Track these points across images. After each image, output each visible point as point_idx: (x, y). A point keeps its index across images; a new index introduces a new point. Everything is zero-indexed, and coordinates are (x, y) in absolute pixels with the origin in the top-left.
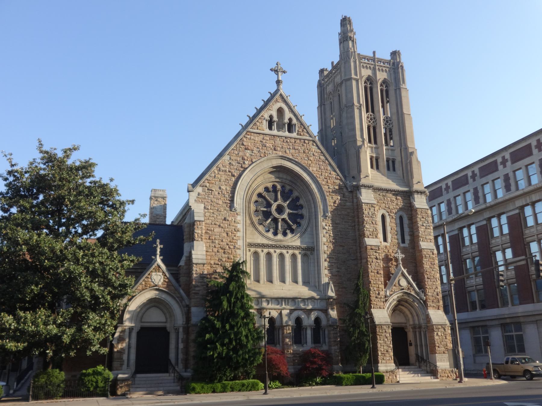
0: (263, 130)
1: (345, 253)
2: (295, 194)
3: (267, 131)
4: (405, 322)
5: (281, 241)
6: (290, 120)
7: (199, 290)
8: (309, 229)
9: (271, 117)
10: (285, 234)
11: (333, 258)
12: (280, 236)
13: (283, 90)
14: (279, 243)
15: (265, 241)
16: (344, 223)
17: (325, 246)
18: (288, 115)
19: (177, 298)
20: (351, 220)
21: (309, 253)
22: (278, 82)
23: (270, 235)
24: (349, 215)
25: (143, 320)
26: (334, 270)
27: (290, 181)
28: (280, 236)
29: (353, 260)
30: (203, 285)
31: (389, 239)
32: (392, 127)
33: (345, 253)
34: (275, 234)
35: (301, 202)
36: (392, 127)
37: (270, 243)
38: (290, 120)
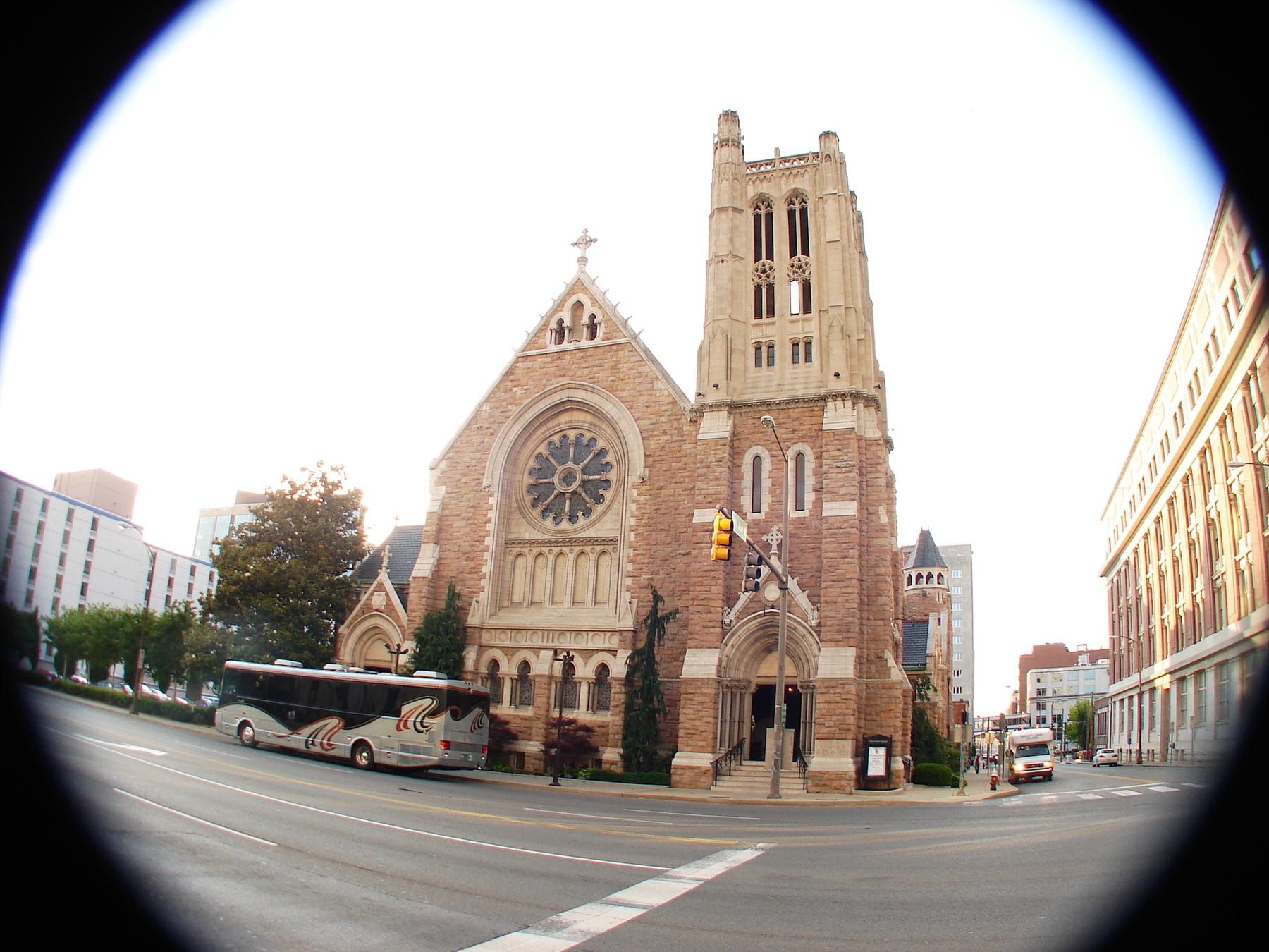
0: (546, 348)
1: (668, 544)
2: (601, 444)
3: (553, 348)
4: (796, 675)
5: (564, 532)
6: (593, 317)
7: (416, 617)
8: (615, 506)
9: (561, 321)
10: (572, 518)
11: (644, 554)
12: (565, 525)
13: (591, 270)
14: (559, 536)
15: (537, 535)
16: (673, 485)
17: (633, 534)
18: (588, 310)
19: (397, 628)
20: (689, 477)
21: (609, 548)
22: (583, 260)
23: (549, 523)
24: (685, 469)
25: (367, 658)
26: (643, 577)
27: (591, 423)
28: (565, 525)
29: (684, 555)
30: (421, 609)
31: (765, 507)
32: (810, 274)
33: (668, 544)
34: (557, 520)
35: (610, 458)
36: (810, 274)
37: (545, 537)
38: (593, 317)
